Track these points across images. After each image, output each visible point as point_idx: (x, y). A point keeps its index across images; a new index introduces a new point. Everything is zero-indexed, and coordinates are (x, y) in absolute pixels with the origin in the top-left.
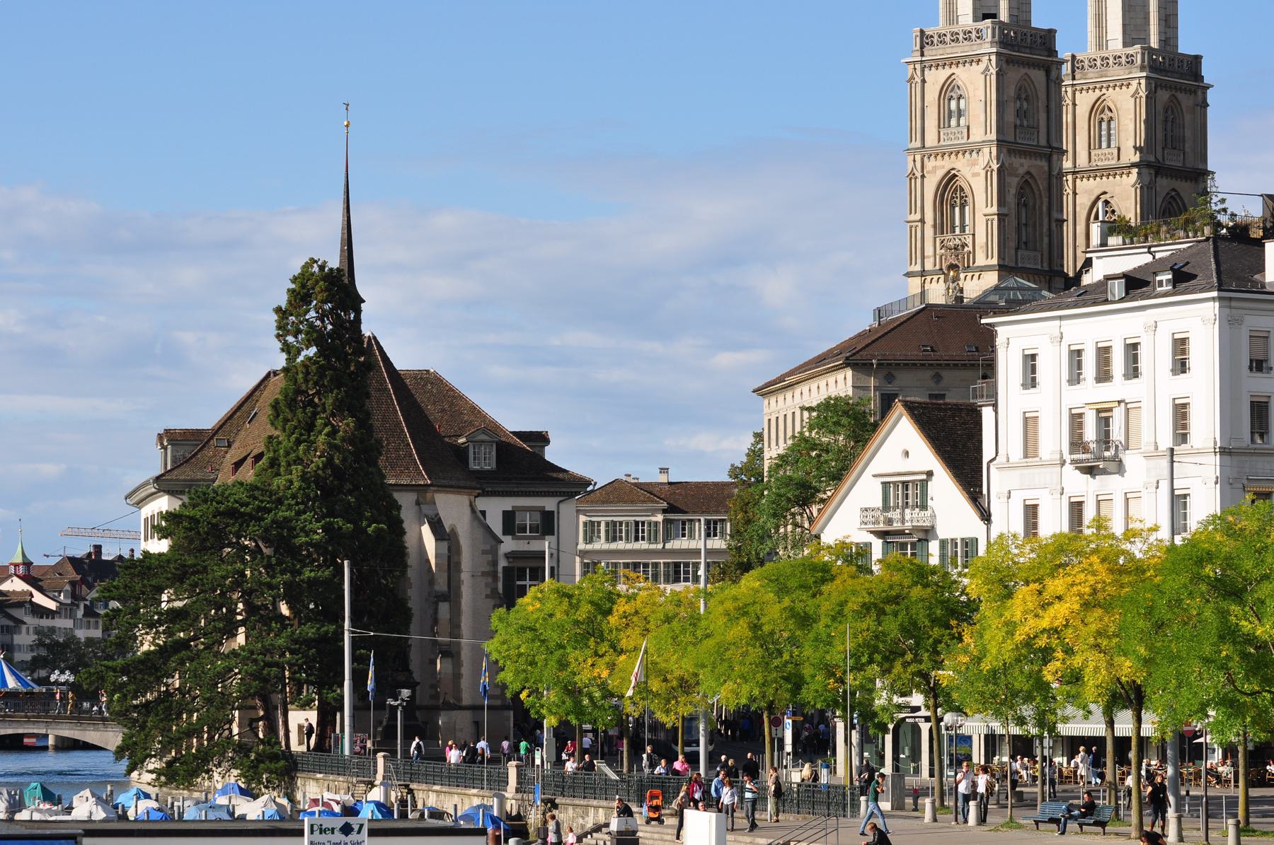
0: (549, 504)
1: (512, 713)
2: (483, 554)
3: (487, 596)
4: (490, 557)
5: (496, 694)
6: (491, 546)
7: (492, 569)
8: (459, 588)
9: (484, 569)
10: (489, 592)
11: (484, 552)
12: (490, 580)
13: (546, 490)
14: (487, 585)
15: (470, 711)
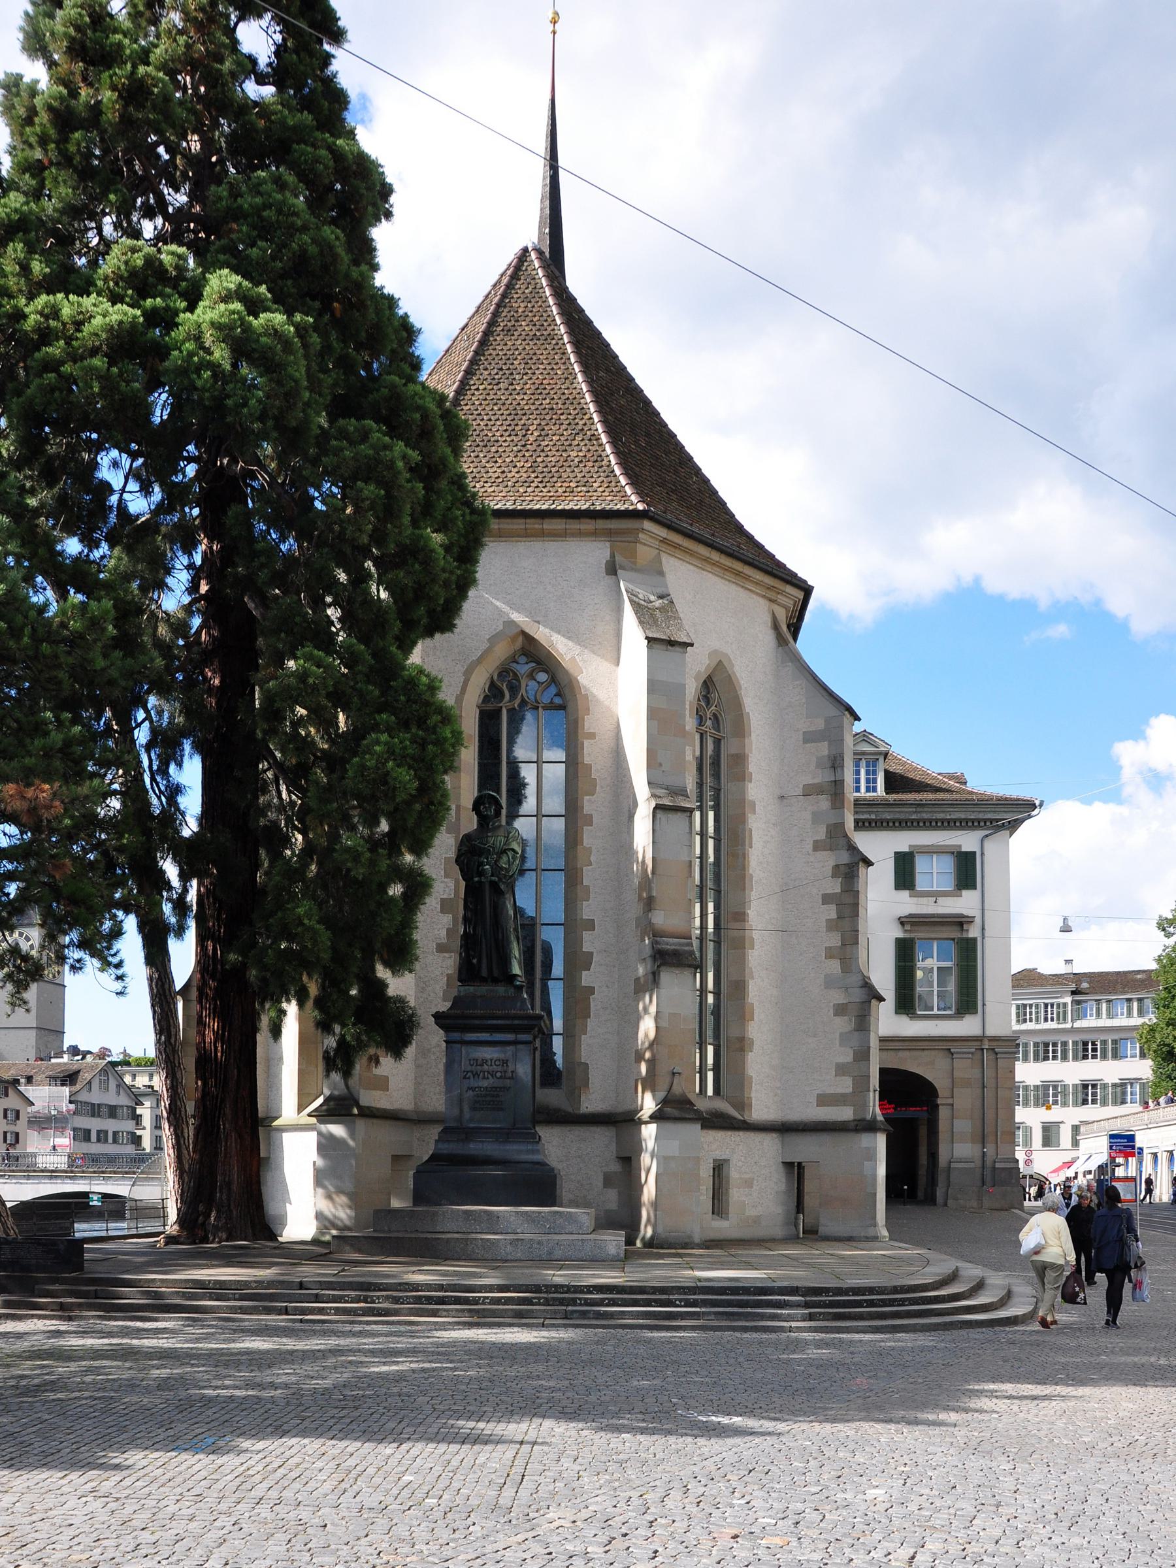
0: (967, 841)
1: (881, 1141)
2: (806, 741)
3: (817, 846)
4: (823, 749)
5: (840, 1090)
6: (828, 721)
7: (828, 776)
8: (741, 819)
9: (809, 780)
10: (821, 834)
11: (810, 738)
12: (824, 803)
13: (963, 816)
14: (816, 817)
15: (774, 1135)
